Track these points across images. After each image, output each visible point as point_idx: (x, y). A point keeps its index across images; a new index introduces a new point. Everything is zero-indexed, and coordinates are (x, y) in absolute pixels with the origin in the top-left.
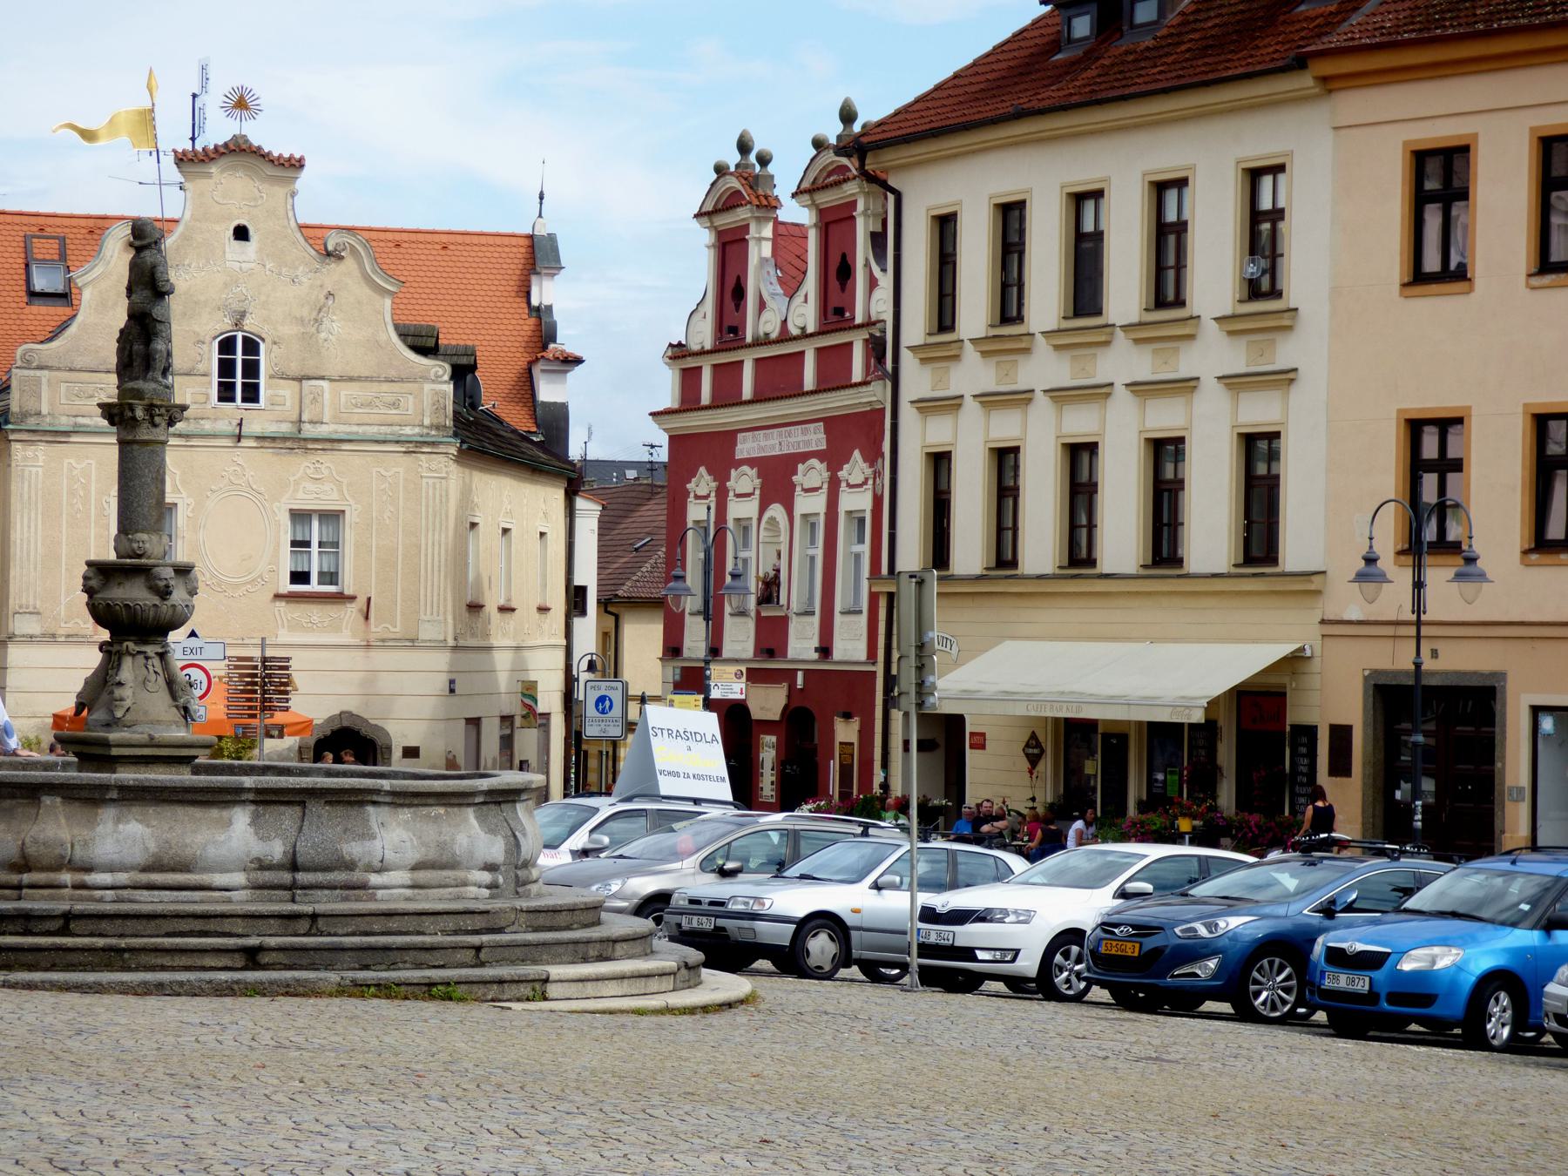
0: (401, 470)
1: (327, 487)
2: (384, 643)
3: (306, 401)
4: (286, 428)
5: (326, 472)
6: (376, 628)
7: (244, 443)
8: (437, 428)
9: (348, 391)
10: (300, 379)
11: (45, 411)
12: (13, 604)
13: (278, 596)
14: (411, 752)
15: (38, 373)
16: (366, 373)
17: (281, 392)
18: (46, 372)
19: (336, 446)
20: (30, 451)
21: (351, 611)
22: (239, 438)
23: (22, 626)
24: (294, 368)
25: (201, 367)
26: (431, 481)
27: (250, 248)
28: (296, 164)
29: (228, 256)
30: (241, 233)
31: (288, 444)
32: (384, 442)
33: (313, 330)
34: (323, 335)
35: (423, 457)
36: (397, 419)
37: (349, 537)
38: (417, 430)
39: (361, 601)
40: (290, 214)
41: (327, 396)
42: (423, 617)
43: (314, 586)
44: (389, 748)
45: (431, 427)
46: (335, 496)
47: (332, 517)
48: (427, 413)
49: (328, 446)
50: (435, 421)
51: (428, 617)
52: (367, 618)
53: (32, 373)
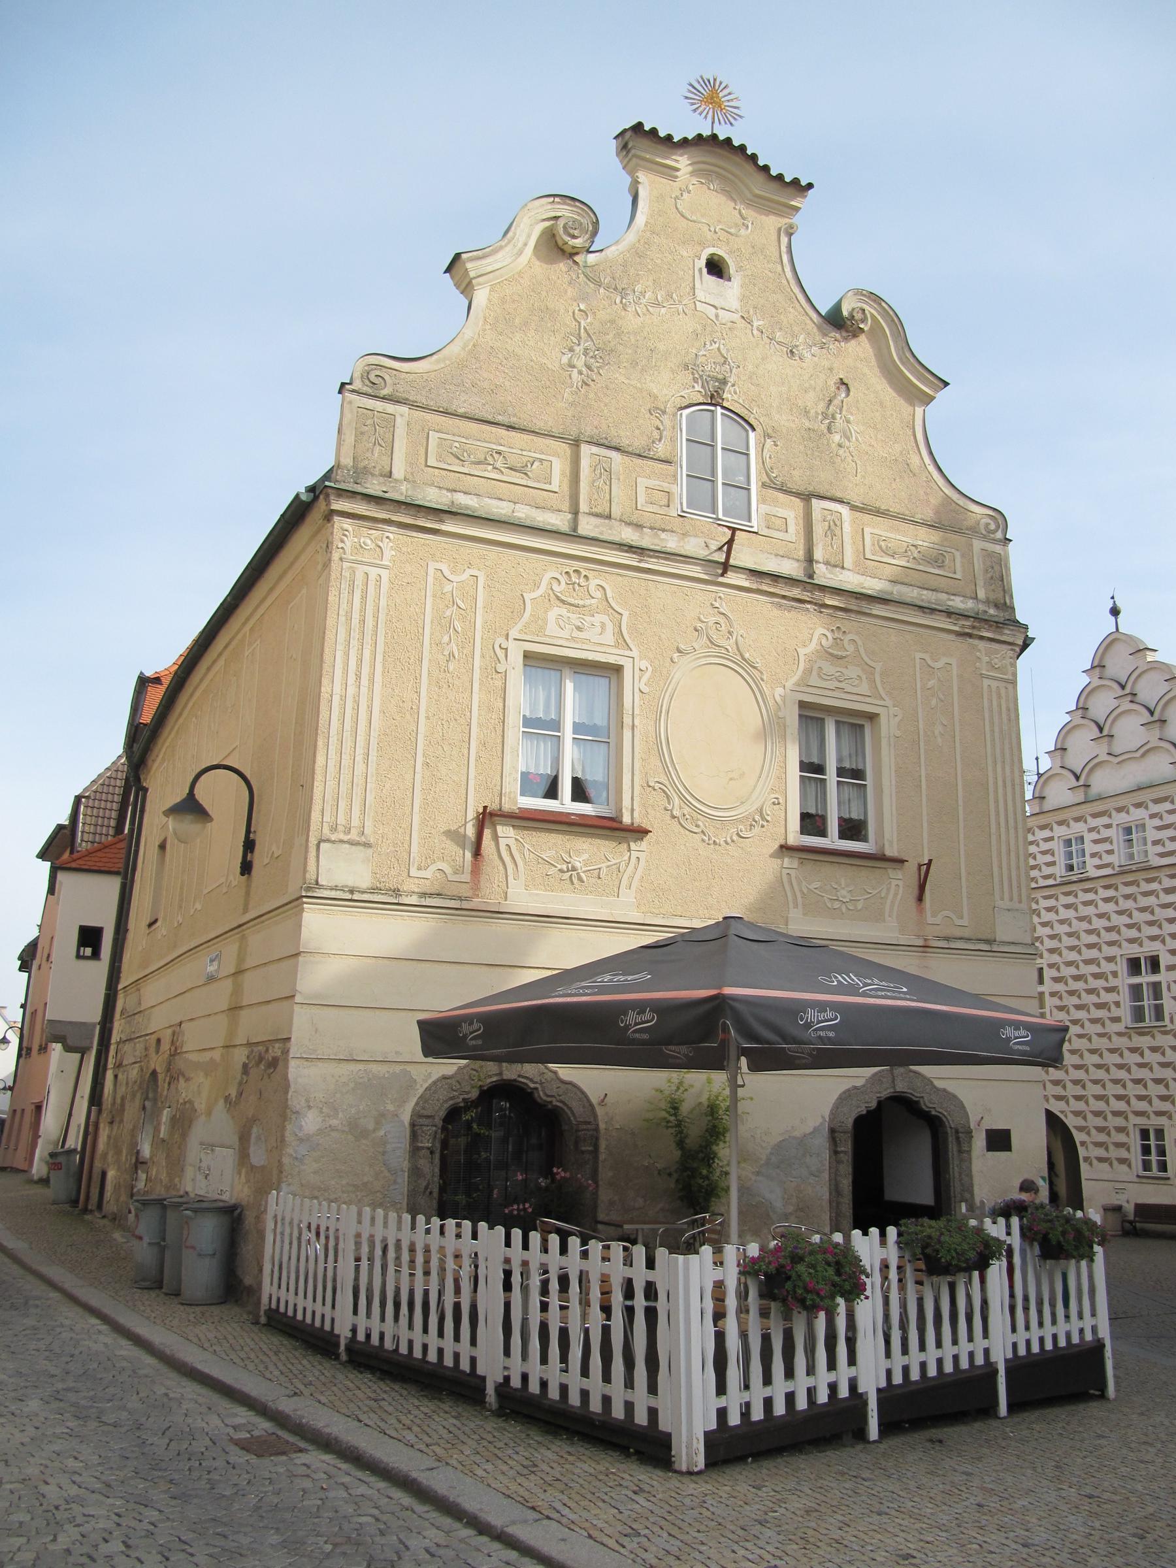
0: (953, 661)
1: (853, 672)
2: (950, 944)
3: (819, 530)
4: (790, 568)
5: (851, 648)
6: (936, 917)
7: (732, 578)
8: (996, 606)
9: (875, 528)
10: (807, 497)
11: (399, 472)
12: (320, 819)
13: (785, 849)
14: (999, 1140)
15: (390, 408)
16: (895, 508)
17: (782, 512)
18: (404, 409)
19: (865, 606)
20: (368, 537)
21: (900, 883)
22: (726, 567)
23: (337, 867)
24: (798, 480)
25: (661, 449)
26: (994, 684)
27: (729, 293)
28: (799, 188)
29: (700, 295)
30: (716, 267)
31: (796, 592)
32: (933, 611)
33: (824, 427)
34: (837, 438)
35: (982, 645)
36: (943, 583)
37: (884, 761)
38: (970, 604)
39: (911, 867)
40: (785, 258)
41: (847, 527)
42: (999, 903)
43: (832, 840)
44: (969, 1133)
45: (987, 602)
46: (864, 688)
47: (855, 723)
48: (980, 583)
49: (853, 604)
50: (992, 597)
51: (1006, 904)
52: (920, 898)
53: (379, 405)
